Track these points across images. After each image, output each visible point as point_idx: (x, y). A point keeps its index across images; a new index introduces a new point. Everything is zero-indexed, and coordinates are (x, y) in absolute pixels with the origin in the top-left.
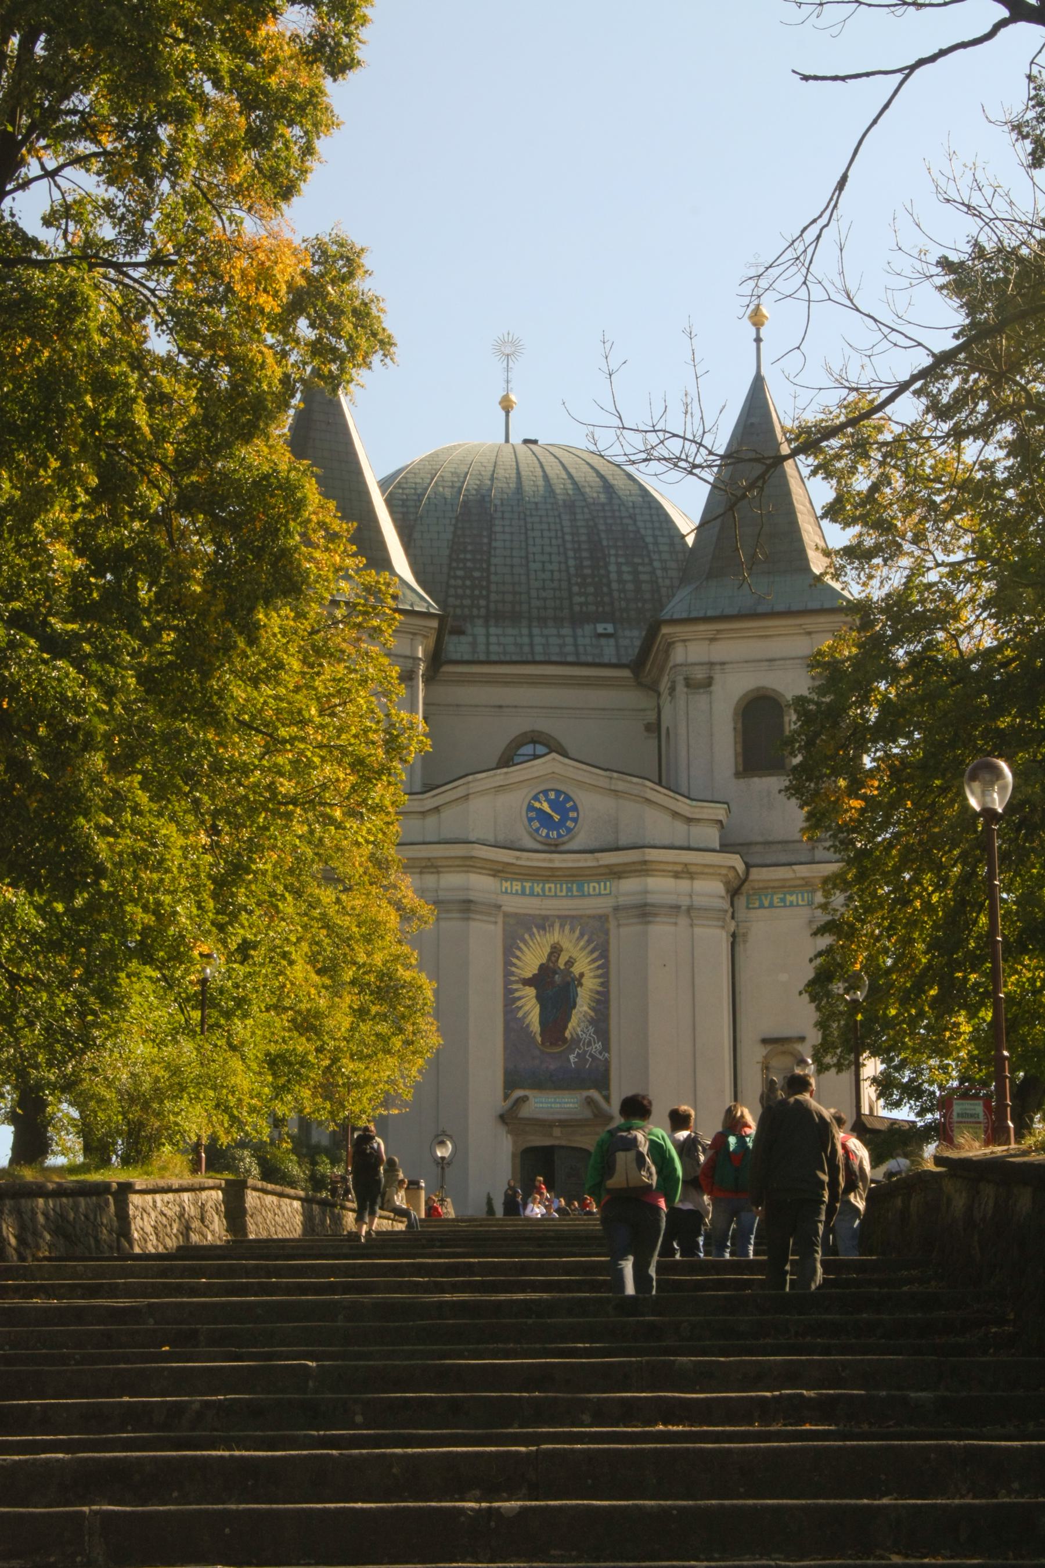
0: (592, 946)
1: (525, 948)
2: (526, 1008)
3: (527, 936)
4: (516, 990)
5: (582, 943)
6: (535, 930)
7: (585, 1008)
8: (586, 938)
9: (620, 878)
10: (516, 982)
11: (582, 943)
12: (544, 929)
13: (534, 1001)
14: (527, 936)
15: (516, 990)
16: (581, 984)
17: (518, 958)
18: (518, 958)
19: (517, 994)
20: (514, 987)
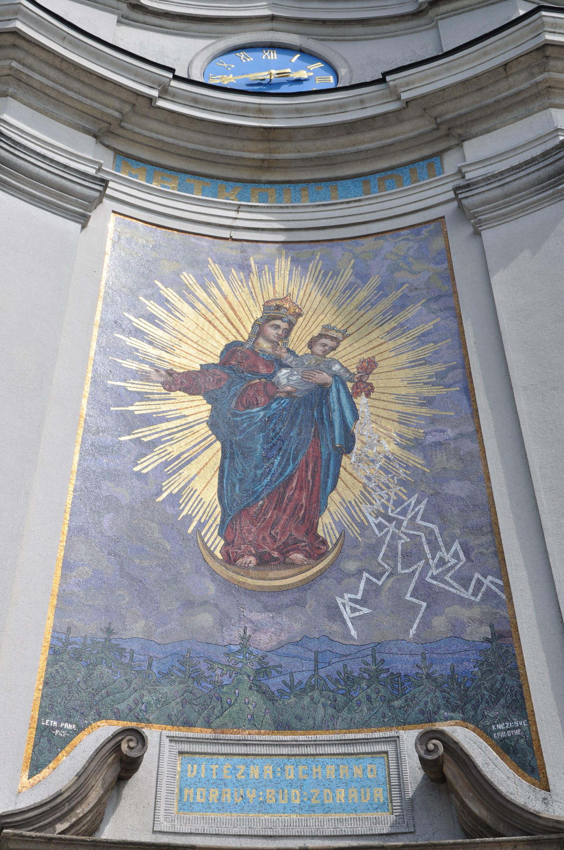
0: (394, 296)
1: (185, 307)
2: (175, 450)
3: (188, 278)
4: (143, 397)
5: (362, 295)
6: (214, 268)
7: (389, 447)
8: (374, 281)
9: (462, 139)
10: (145, 377)
11: (362, 295)
12: (245, 268)
13: (204, 429)
14: (188, 278)
15: (143, 397)
16: (369, 391)
17: (152, 319)
18: (152, 319)
19: (139, 408)
20: (134, 386)
